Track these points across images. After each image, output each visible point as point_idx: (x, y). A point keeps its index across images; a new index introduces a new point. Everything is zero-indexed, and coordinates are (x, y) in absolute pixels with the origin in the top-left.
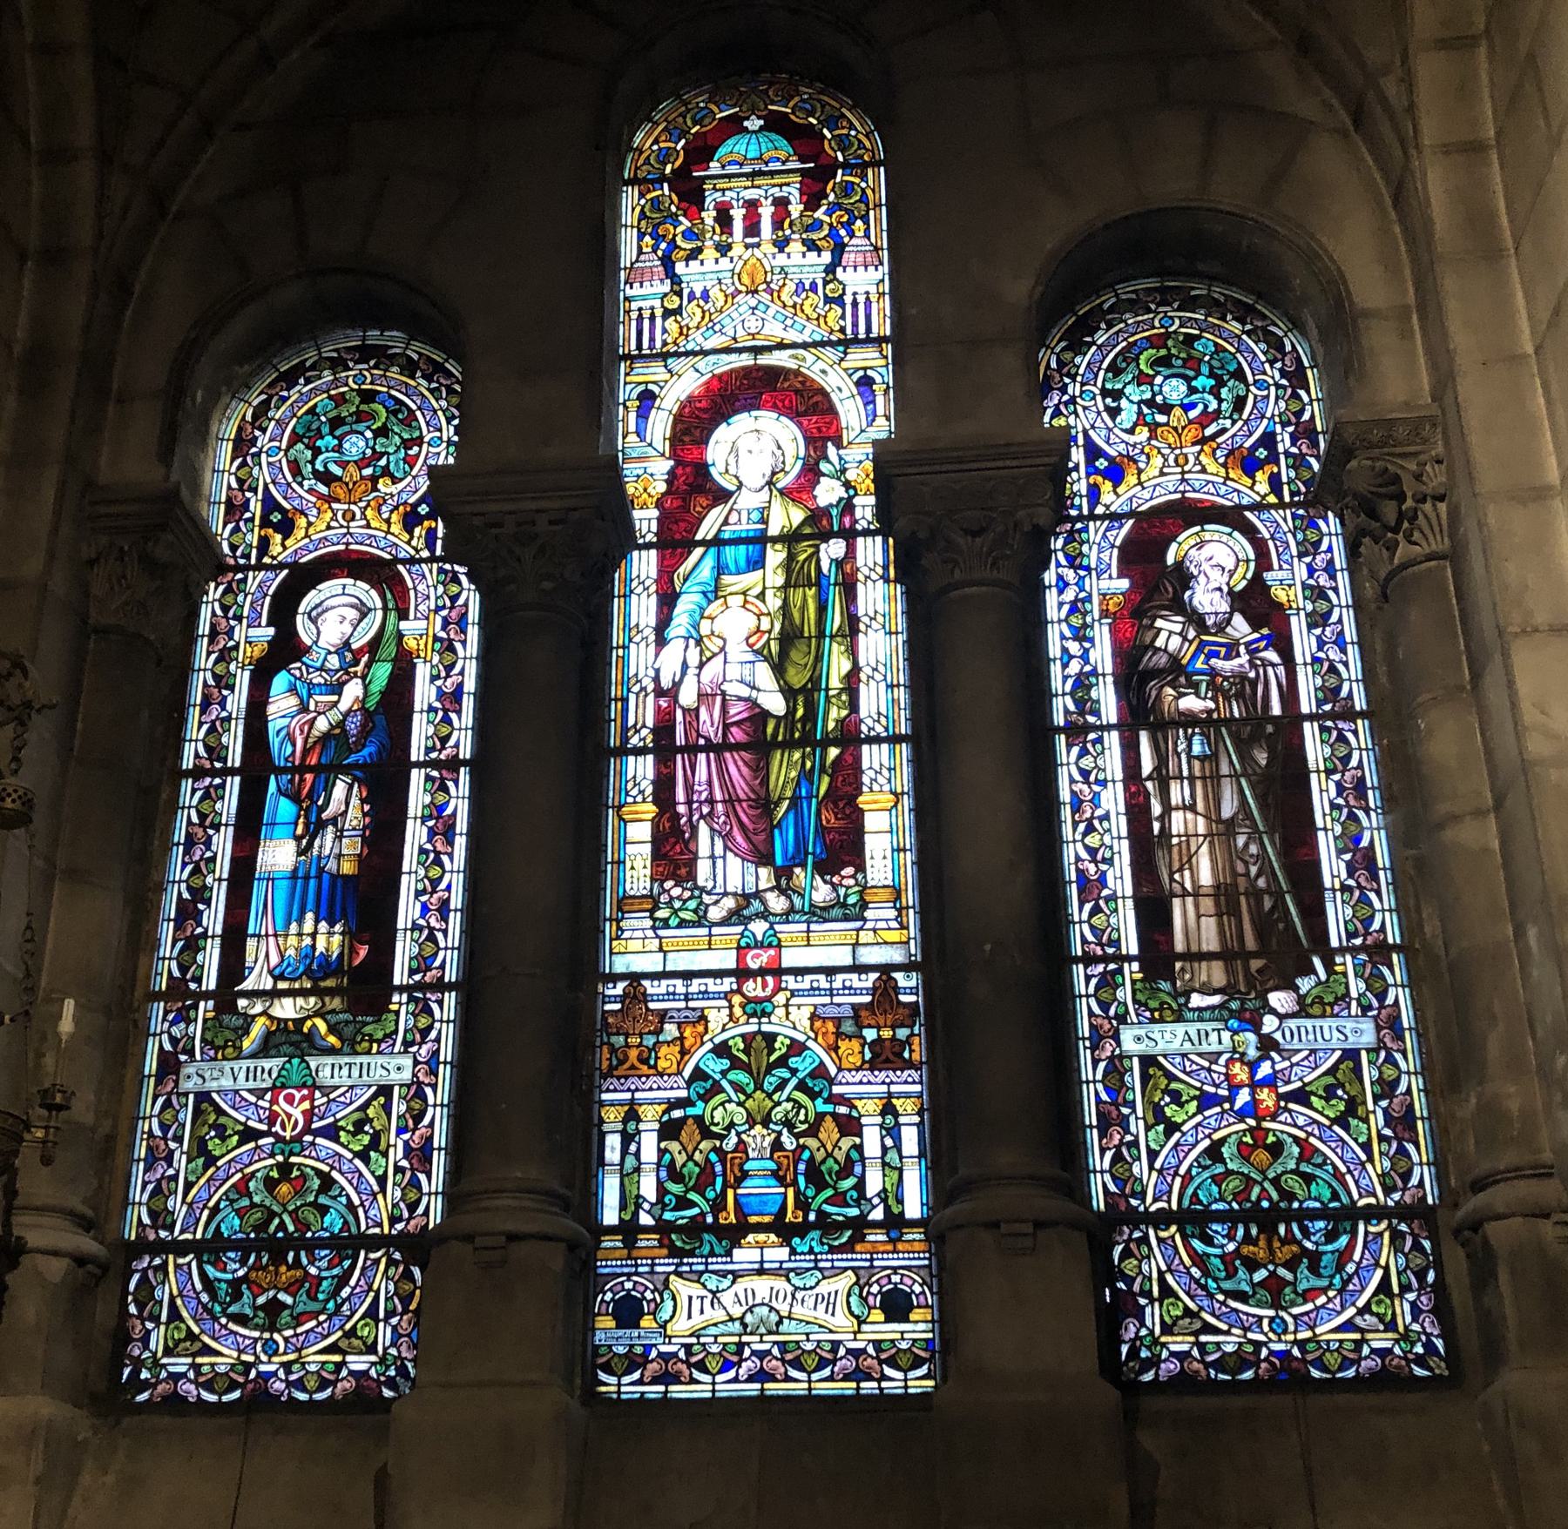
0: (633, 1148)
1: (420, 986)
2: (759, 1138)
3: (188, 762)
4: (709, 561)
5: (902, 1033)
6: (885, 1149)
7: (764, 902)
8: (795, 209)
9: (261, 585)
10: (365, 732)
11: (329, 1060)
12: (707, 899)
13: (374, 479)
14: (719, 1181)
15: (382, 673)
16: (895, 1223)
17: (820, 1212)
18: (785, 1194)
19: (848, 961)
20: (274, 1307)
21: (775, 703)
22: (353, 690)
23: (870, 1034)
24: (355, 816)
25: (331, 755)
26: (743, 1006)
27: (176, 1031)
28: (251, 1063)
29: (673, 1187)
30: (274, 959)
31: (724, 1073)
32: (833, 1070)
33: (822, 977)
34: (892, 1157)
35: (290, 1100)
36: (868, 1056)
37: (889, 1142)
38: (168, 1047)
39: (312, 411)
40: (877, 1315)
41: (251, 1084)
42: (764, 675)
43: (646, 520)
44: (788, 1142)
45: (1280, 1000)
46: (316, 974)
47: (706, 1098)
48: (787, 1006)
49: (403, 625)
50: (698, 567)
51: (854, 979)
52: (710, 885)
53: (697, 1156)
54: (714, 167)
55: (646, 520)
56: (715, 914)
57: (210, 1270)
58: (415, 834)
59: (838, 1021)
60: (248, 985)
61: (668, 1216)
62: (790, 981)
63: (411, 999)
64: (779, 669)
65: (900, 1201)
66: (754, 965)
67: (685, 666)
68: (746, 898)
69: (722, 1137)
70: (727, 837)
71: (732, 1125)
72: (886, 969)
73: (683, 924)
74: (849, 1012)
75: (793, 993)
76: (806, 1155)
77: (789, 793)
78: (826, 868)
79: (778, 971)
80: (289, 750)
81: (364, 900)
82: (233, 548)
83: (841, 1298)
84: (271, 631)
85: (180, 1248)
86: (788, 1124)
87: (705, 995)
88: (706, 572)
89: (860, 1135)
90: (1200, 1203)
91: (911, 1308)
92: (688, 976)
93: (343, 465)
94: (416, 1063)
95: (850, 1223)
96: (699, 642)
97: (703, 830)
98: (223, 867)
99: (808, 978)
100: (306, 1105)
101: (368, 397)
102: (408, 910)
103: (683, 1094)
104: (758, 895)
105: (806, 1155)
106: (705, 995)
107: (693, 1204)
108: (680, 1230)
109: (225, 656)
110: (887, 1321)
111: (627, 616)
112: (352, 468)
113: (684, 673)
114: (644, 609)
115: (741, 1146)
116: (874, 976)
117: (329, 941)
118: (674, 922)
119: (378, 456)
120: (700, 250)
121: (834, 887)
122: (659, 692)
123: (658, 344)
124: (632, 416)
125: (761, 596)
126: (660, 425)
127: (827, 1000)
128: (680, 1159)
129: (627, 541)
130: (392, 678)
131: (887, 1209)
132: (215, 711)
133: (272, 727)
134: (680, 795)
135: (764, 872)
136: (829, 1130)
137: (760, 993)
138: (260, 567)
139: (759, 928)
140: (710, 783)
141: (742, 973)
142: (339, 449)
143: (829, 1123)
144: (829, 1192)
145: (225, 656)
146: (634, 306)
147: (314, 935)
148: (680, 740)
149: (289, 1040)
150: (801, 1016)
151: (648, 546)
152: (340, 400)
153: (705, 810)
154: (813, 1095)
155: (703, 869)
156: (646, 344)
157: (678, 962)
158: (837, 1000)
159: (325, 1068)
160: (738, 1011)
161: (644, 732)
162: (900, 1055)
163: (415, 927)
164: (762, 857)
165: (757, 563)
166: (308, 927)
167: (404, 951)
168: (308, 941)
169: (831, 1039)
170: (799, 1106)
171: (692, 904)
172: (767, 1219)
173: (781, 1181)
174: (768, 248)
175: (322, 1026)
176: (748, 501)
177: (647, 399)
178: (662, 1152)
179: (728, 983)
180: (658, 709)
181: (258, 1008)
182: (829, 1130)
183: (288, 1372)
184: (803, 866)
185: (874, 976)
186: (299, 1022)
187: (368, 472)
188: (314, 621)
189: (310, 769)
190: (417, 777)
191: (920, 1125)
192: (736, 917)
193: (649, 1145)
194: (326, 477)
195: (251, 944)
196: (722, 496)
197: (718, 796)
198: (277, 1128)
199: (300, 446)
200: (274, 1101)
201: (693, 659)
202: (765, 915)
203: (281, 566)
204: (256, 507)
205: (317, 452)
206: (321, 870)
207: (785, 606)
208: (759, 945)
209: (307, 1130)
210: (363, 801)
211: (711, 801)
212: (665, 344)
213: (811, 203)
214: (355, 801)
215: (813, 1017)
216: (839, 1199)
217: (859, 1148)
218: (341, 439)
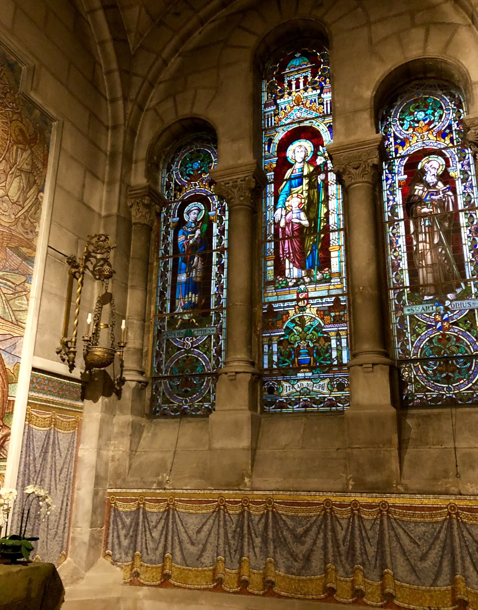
0: (271, 348)
1: (216, 309)
2: (303, 344)
3: (160, 255)
4: (288, 185)
5: (342, 313)
6: (337, 345)
7: (304, 280)
8: (309, 79)
10: (201, 242)
11: (196, 329)
12: (288, 280)
13: (201, 174)
14: (293, 356)
15: (205, 226)
16: (341, 365)
17: (320, 364)
18: (310, 359)
19: (327, 294)
20: (186, 391)
21: (305, 223)
22: (198, 232)
23: (333, 314)
24: (200, 266)
26: (298, 309)
27: (161, 324)
28: (178, 331)
29: (281, 358)
30: (183, 304)
31: (294, 327)
32: (323, 325)
33: (319, 299)
34: (339, 348)
35: (188, 340)
36: (332, 320)
37: (338, 343)
38: (159, 328)
39: (185, 157)
40: (335, 390)
41: (179, 336)
42: (303, 215)
43: (270, 175)
44: (311, 345)
45: (450, 296)
46: (191, 306)
47: (289, 334)
48: (310, 308)
49: (210, 213)
50: (285, 187)
51: (328, 300)
52: (289, 276)
53: (287, 350)
54: (287, 71)
55: (270, 175)
56: (290, 284)
57: (171, 383)
58: (215, 269)
59: (324, 311)
60: (177, 311)
61: (280, 365)
62: (311, 301)
63: (215, 312)
64: (307, 214)
65: (342, 359)
66: (301, 297)
67: (282, 215)
68: (298, 279)
69: (293, 344)
70: (294, 263)
71: (296, 341)
72: (337, 296)
73: (283, 288)
74: (327, 308)
75: (312, 304)
76: (316, 348)
77: (310, 249)
78: (320, 269)
79: (307, 298)
80: (183, 250)
81: (202, 287)
82: (168, 197)
83: (326, 385)
84: (178, 218)
85: (165, 378)
86: (311, 340)
87: (288, 306)
88: (287, 188)
89: (330, 342)
90: (426, 355)
91: (345, 388)
92: (284, 302)
93: (193, 171)
94: (217, 329)
95: (328, 365)
96: (285, 209)
97: (287, 261)
98: (170, 282)
99: (316, 300)
100: (191, 341)
101: (199, 151)
102: (214, 289)
103: (283, 333)
104: (302, 278)
105: (316, 348)
106: (288, 306)
107: (286, 362)
108: (283, 369)
109: (168, 227)
110: (338, 391)
111: (266, 203)
112: (195, 172)
113: (281, 217)
114: (270, 201)
115: (299, 346)
116: (334, 298)
117: (194, 298)
118: (280, 287)
119: (201, 168)
120: (283, 95)
121: (323, 274)
122: (275, 224)
123: (273, 124)
124: (266, 146)
125: (302, 193)
126: (274, 148)
127: (321, 306)
128: (283, 350)
129: (266, 182)
130: (208, 227)
131: (338, 361)
132: (166, 242)
133: (179, 244)
134: (281, 252)
135: (303, 272)
136: (322, 342)
137: (303, 305)
138: (174, 202)
139: (302, 287)
140: (289, 248)
141: (298, 300)
142: (192, 167)
143: (322, 339)
144: (322, 358)
145: (168, 227)
146: (266, 114)
147: (191, 298)
148: (281, 237)
149: (187, 324)
150: (314, 311)
151: (271, 183)
152: (192, 153)
153: (288, 256)
154: (317, 332)
155: (287, 272)
156: (270, 125)
157: (282, 298)
158: (324, 305)
159: (195, 331)
160: (297, 310)
161: (271, 236)
162: (341, 319)
163: (216, 294)
164: (302, 267)
165: (301, 184)
166: (190, 295)
167: (213, 300)
168: (190, 299)
169: (322, 316)
170: (313, 335)
171: (284, 282)
172: (306, 365)
173: (310, 355)
174: (302, 91)
175: (194, 321)
176: (298, 166)
177: (270, 141)
178: (278, 349)
179: (294, 303)
180: (275, 228)
181: (180, 317)
182: (322, 342)
183: (190, 407)
184: (314, 269)
185: (334, 298)
186: (189, 320)
187: (199, 172)
188: (188, 214)
189: (189, 254)
190: (214, 254)
191: (347, 338)
192: (296, 285)
193: (275, 348)
194: (189, 175)
195: (177, 301)
196: (291, 166)
197: (291, 251)
198: (185, 347)
199: (183, 168)
200: (184, 340)
201: (284, 214)
202: (304, 283)
203: (180, 201)
204: (173, 185)
205: (187, 168)
206: (192, 281)
207: (308, 196)
208: (302, 292)
209: (192, 347)
210: (202, 261)
211: (289, 253)
212: (275, 124)
213: (314, 76)
214: (200, 262)
215: (317, 311)
216: (325, 359)
217: (330, 345)
218: (192, 164)
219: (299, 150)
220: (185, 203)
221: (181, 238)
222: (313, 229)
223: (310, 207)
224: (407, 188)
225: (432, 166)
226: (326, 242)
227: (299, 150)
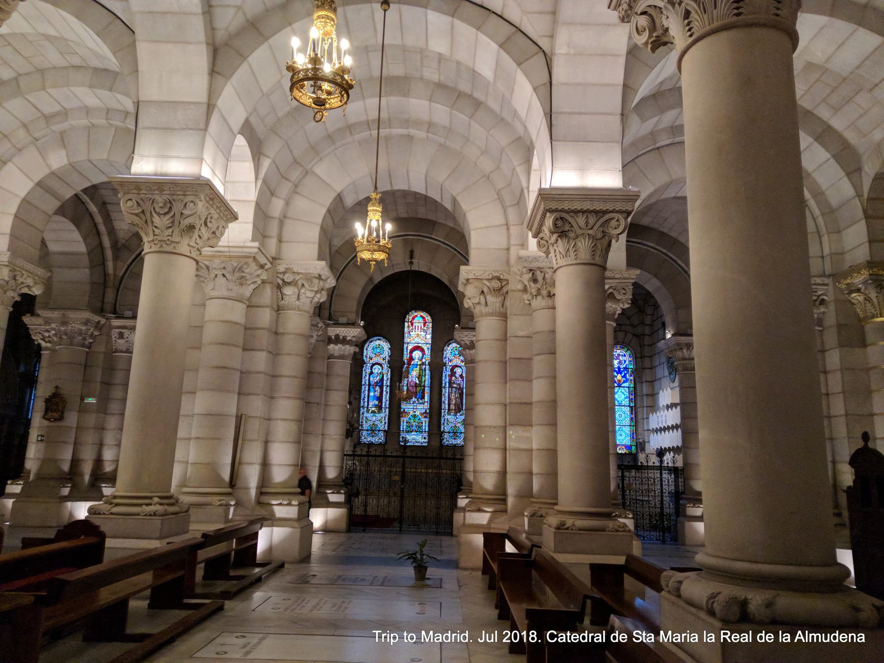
9: (369, 365)
25: (376, 384)
46: (376, 406)
58: (384, 393)
81: (380, 399)
102: (384, 400)
117: (377, 403)
149: (373, 412)
219: (417, 354)
220: (373, 365)
221: (371, 379)
222: (420, 385)
223: (420, 377)
224: (451, 376)
225: (458, 371)
226: (424, 390)
227: (417, 354)
